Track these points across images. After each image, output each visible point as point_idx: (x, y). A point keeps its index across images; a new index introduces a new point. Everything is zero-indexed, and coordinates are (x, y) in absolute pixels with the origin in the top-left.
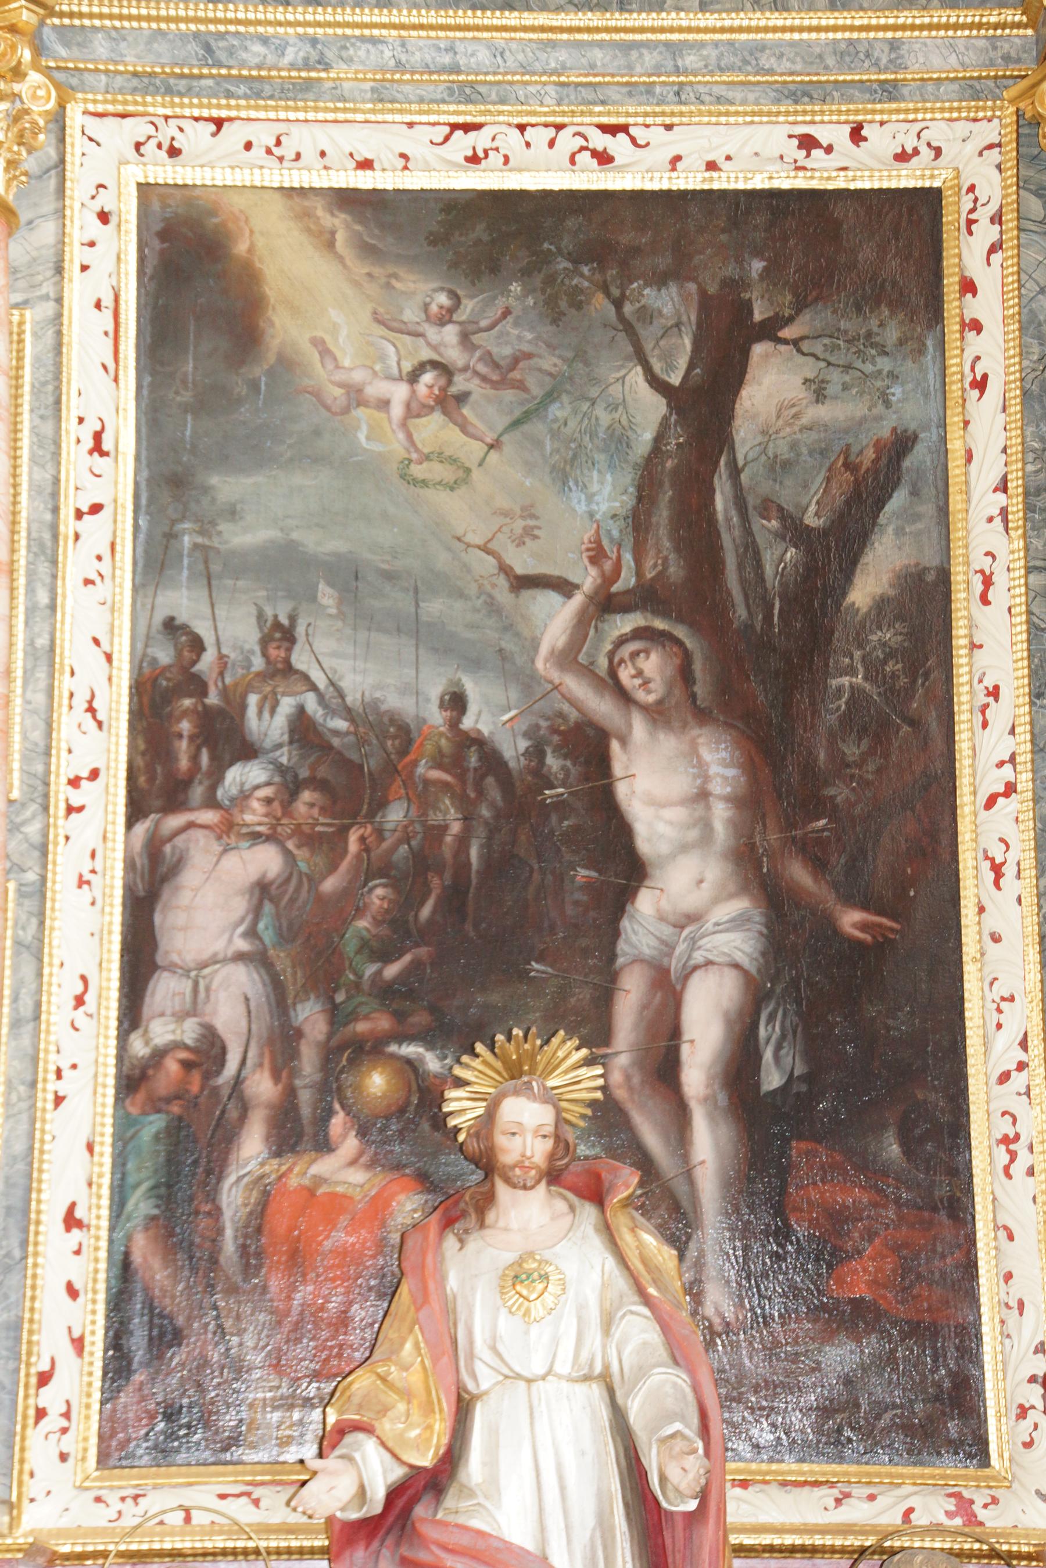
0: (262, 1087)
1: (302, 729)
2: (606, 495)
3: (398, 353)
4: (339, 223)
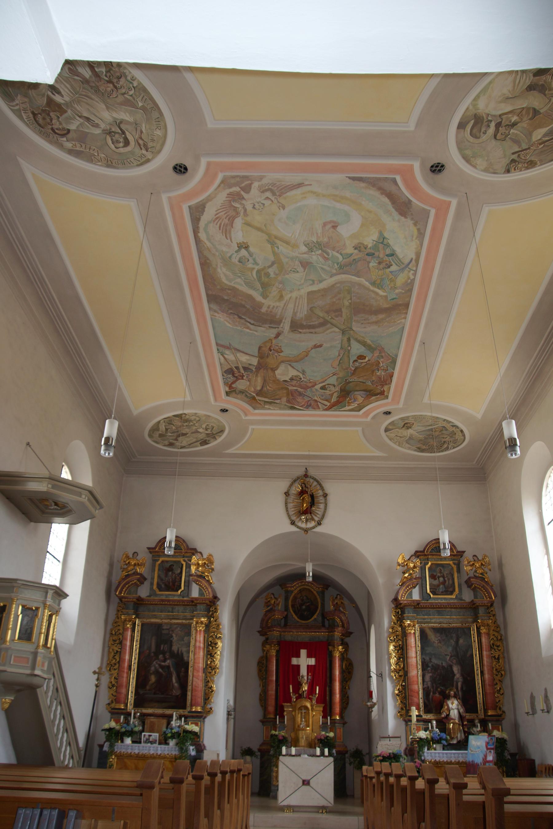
0: (432, 690)
1: (432, 665)
2: (450, 649)
3: (436, 639)
4: (432, 630)
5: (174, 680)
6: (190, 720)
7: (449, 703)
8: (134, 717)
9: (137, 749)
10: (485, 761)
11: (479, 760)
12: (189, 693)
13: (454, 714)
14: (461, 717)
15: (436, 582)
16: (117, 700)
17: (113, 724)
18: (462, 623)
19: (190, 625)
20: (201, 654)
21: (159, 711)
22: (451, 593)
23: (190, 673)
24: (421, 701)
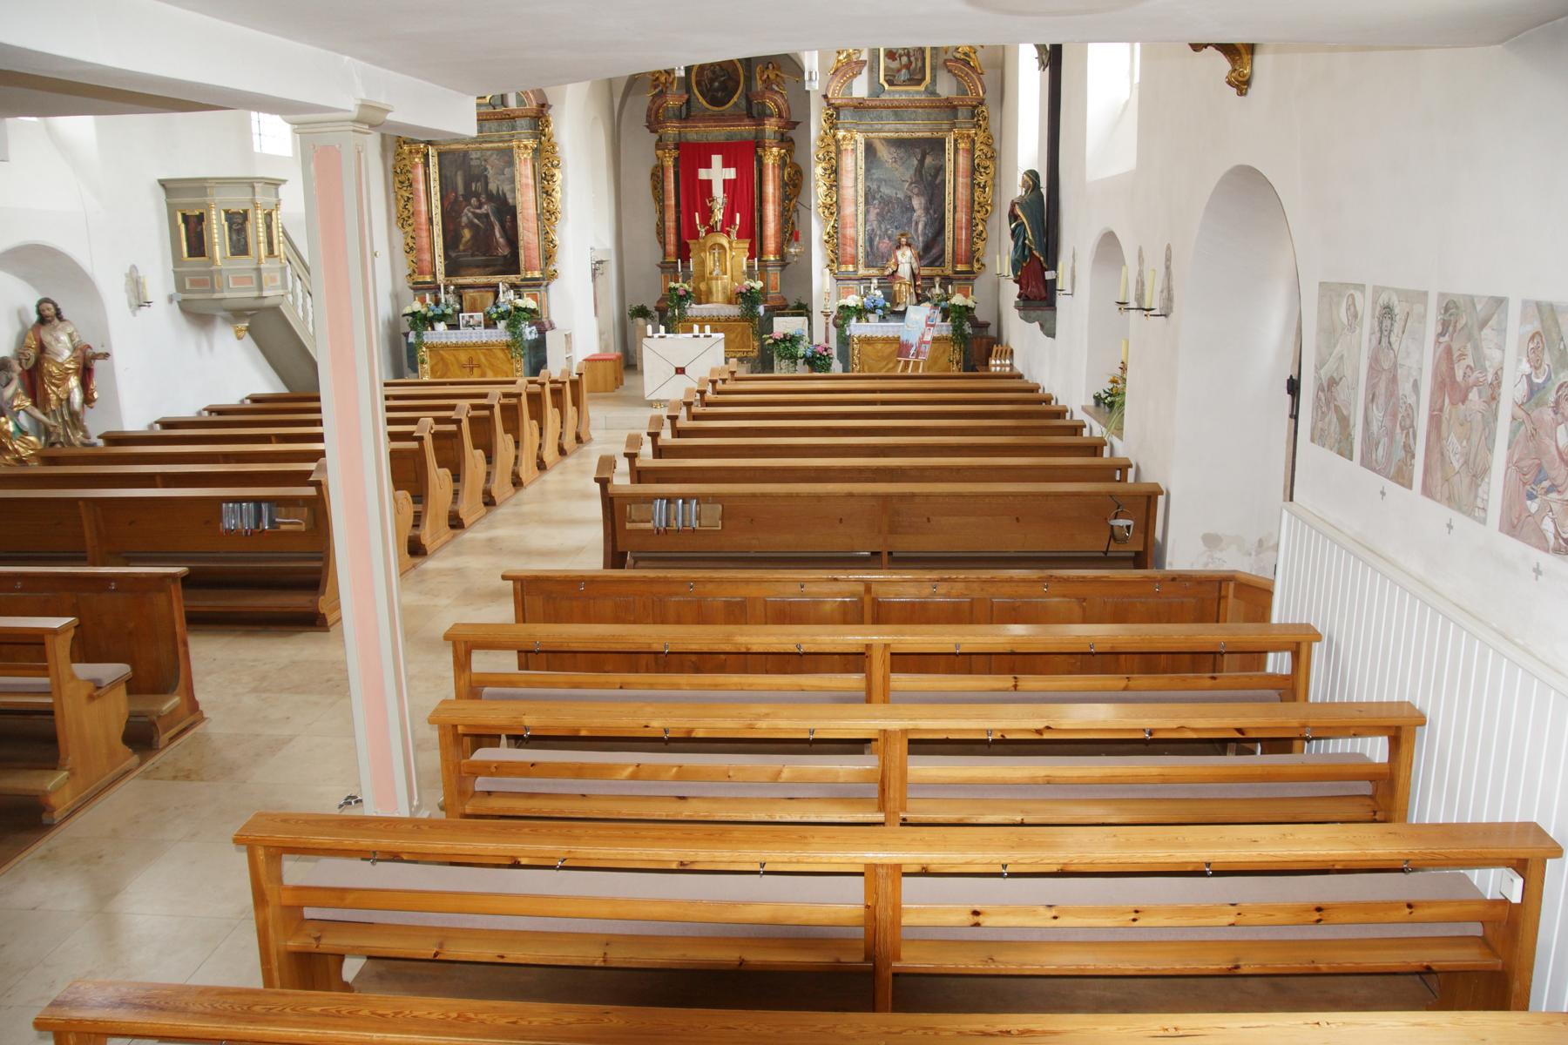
2: (912, 172)
5: (498, 234)
6: (525, 292)
7: (899, 253)
8: (447, 292)
9: (454, 337)
10: (922, 342)
11: (913, 340)
12: (521, 252)
13: (904, 271)
14: (914, 276)
15: (895, 65)
16: (417, 268)
17: (417, 306)
18: (932, 131)
19: (511, 149)
20: (531, 194)
21: (482, 280)
22: (919, 82)
23: (520, 222)
24: (861, 250)
